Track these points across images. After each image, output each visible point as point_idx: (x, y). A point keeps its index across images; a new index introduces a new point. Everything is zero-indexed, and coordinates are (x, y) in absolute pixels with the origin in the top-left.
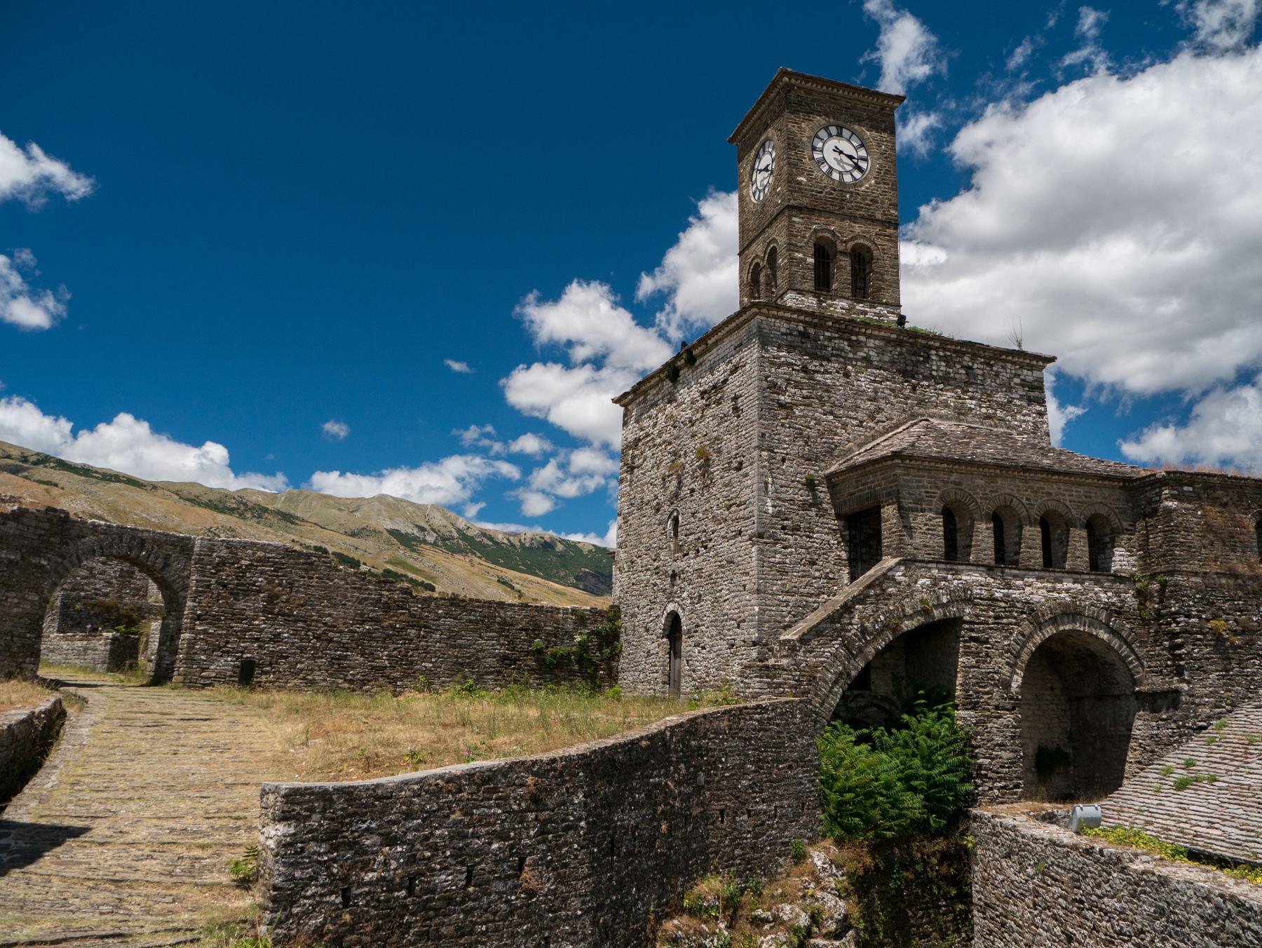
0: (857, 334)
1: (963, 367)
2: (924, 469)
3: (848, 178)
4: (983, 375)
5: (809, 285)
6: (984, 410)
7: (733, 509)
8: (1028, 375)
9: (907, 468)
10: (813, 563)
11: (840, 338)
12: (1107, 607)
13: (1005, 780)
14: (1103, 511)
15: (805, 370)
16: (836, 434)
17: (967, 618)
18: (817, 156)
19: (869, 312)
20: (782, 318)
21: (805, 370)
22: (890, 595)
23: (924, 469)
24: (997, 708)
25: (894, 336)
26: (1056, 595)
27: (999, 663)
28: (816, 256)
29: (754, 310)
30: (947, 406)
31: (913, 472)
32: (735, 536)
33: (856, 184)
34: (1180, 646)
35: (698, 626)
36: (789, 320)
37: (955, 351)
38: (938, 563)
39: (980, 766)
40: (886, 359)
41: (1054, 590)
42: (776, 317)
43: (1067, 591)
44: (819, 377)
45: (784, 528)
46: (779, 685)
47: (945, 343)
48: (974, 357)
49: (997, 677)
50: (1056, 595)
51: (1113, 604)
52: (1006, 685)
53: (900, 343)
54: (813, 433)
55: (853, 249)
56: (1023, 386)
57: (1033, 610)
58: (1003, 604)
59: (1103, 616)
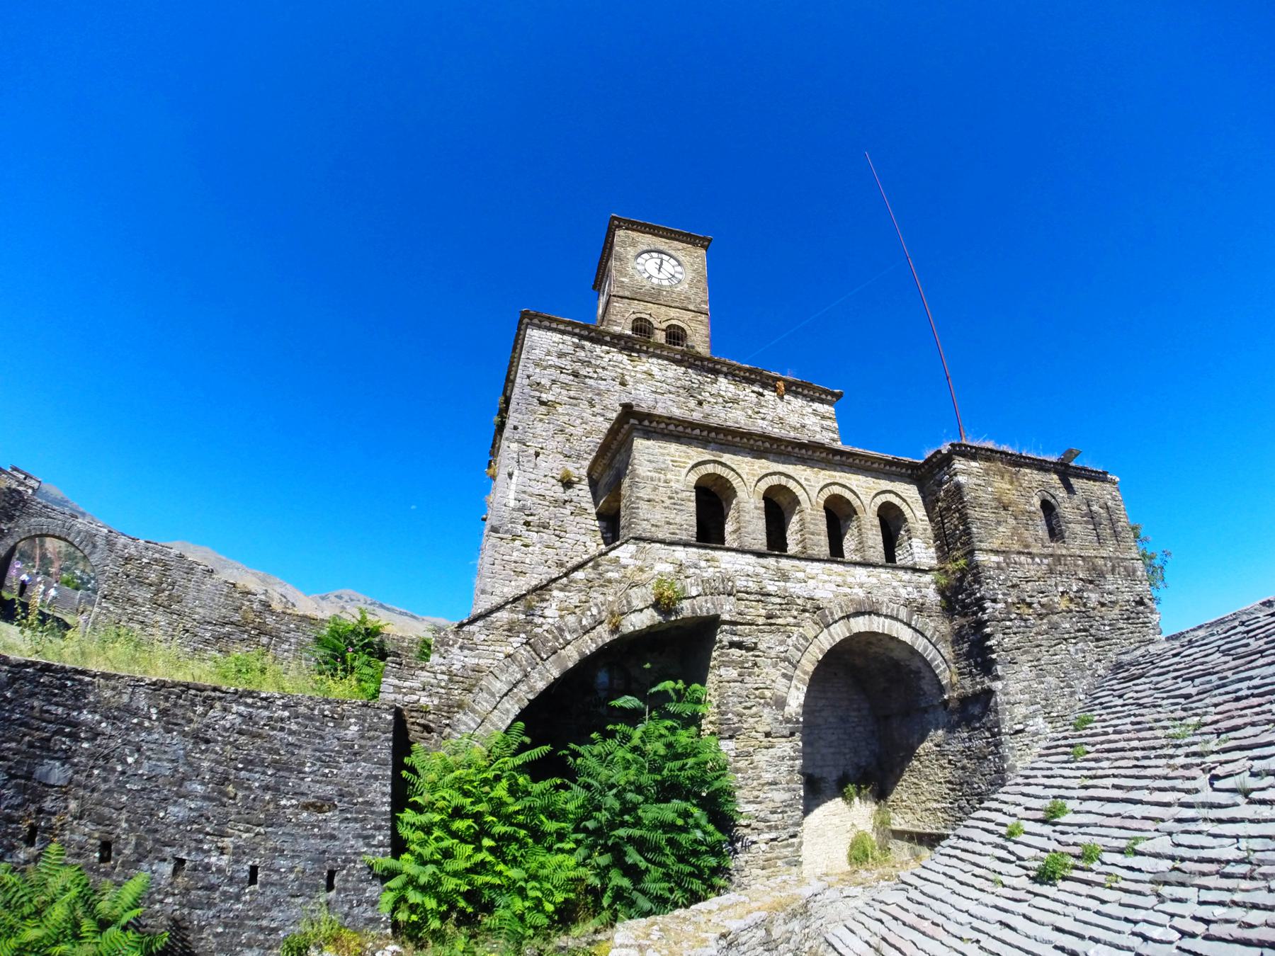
3: (665, 283)
13: (776, 828)
14: (896, 501)
15: (576, 374)
17: (726, 617)
21: (576, 374)
22: (610, 581)
24: (768, 735)
25: (678, 357)
26: (848, 591)
27: (770, 675)
38: (686, 544)
46: (412, 691)
49: (768, 693)
50: (848, 591)
51: (915, 600)
52: (781, 703)
54: (578, 431)
55: (669, 327)
57: (819, 608)
58: (778, 600)
59: (903, 614)
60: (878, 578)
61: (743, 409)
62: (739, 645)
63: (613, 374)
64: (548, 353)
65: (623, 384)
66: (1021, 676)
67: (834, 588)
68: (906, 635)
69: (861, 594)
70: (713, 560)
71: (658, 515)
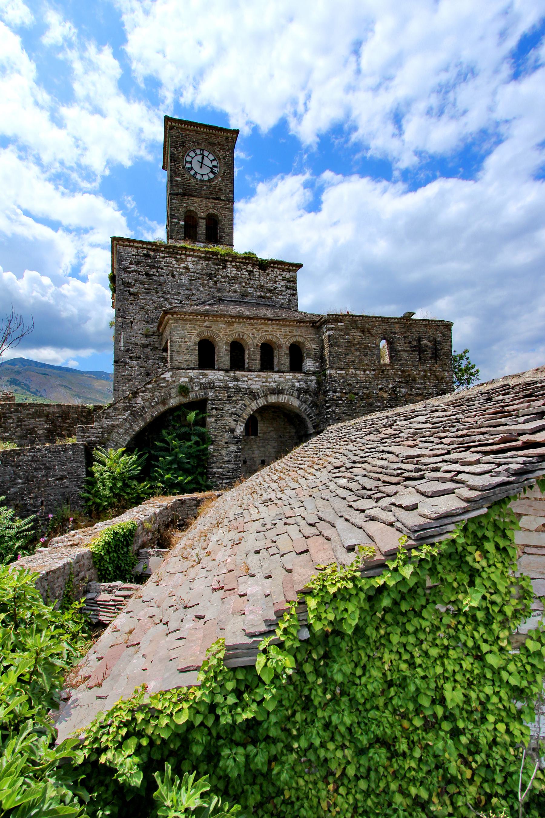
0: (181, 254)
2: (186, 320)
5: (182, 235)
8: (287, 275)
9: (176, 320)
10: (148, 375)
12: (299, 390)
14: (301, 340)
15: (147, 274)
18: (188, 166)
19: (221, 249)
20: (132, 246)
21: (147, 274)
23: (186, 320)
24: (226, 443)
27: (230, 421)
28: (185, 221)
30: (235, 292)
31: (180, 321)
33: (210, 180)
36: (137, 248)
37: (242, 263)
38: (193, 369)
39: (215, 473)
40: (199, 267)
41: (267, 381)
42: (130, 246)
43: (275, 382)
44: (156, 278)
45: (131, 358)
46: (89, 437)
48: (254, 265)
52: (232, 431)
53: (207, 259)
56: (283, 280)
59: (296, 393)
60: (285, 378)
61: (240, 283)
62: (216, 409)
63: (168, 272)
64: (131, 263)
65: (173, 276)
67: (260, 383)
68: (296, 403)
69: (274, 385)
70: (205, 374)
71: (181, 358)
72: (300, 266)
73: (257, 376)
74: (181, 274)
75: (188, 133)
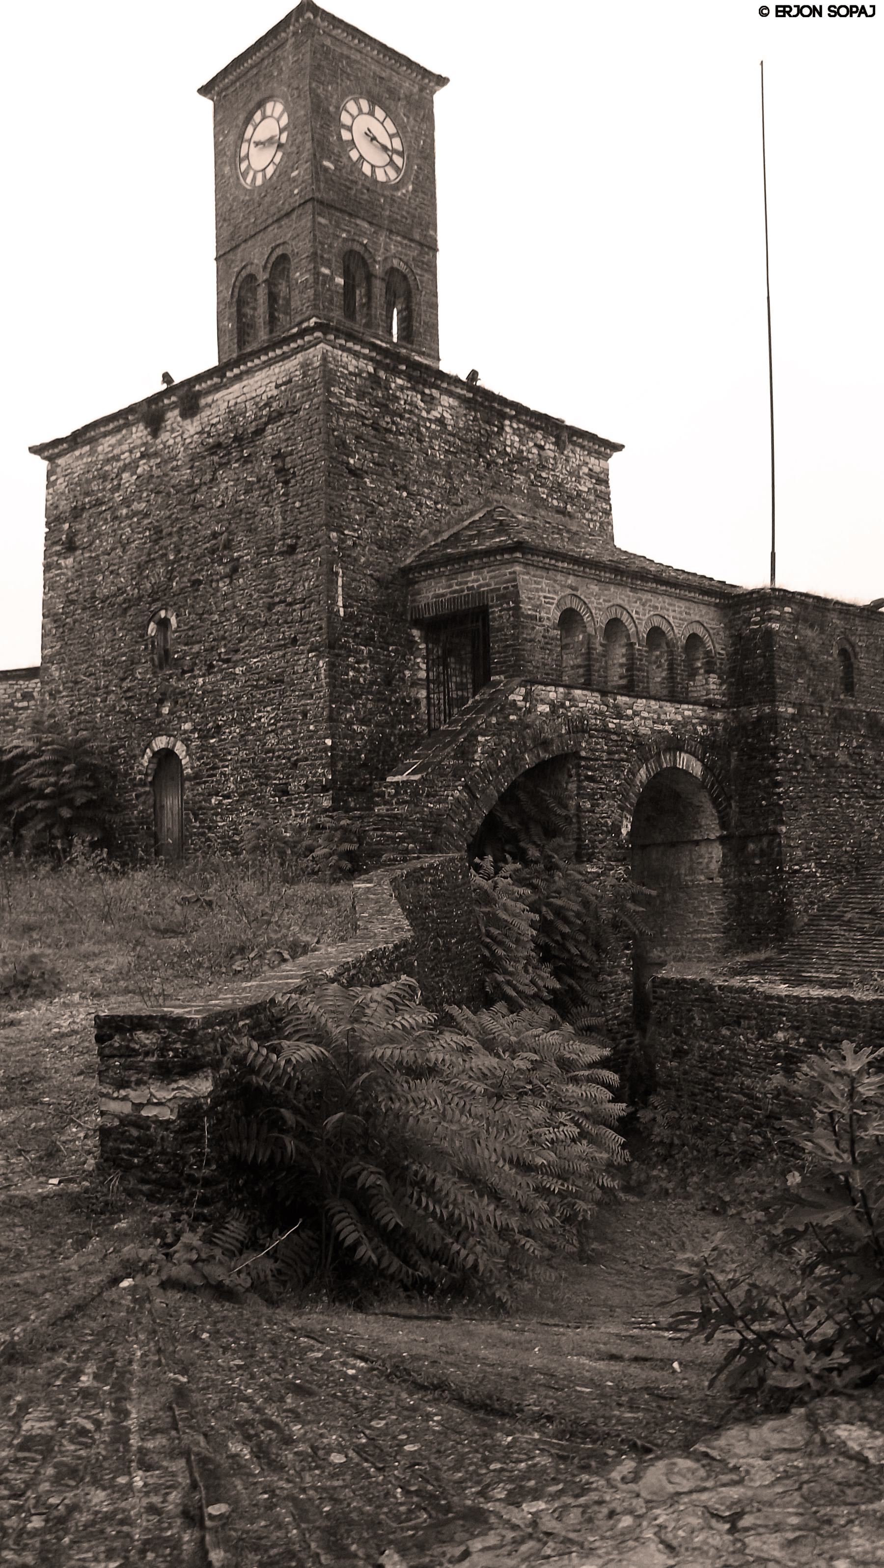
1: (536, 445)
3: (381, 176)
4: (555, 458)
6: (555, 503)
7: (278, 608)
11: (413, 389)
12: (704, 740)
14: (700, 631)
15: (375, 426)
16: (410, 517)
17: (583, 754)
20: (349, 350)
21: (375, 426)
26: (661, 727)
28: (346, 275)
29: (318, 334)
32: (285, 646)
34: (778, 784)
35: (215, 768)
42: (343, 348)
43: (670, 722)
44: (391, 438)
47: (521, 411)
50: (661, 727)
56: (591, 477)
58: (614, 737)
61: (526, 474)
64: (348, 394)
65: (420, 441)
66: (801, 822)
67: (649, 723)
72: (618, 448)
73: (648, 709)
74: (434, 436)
75: (345, 51)
